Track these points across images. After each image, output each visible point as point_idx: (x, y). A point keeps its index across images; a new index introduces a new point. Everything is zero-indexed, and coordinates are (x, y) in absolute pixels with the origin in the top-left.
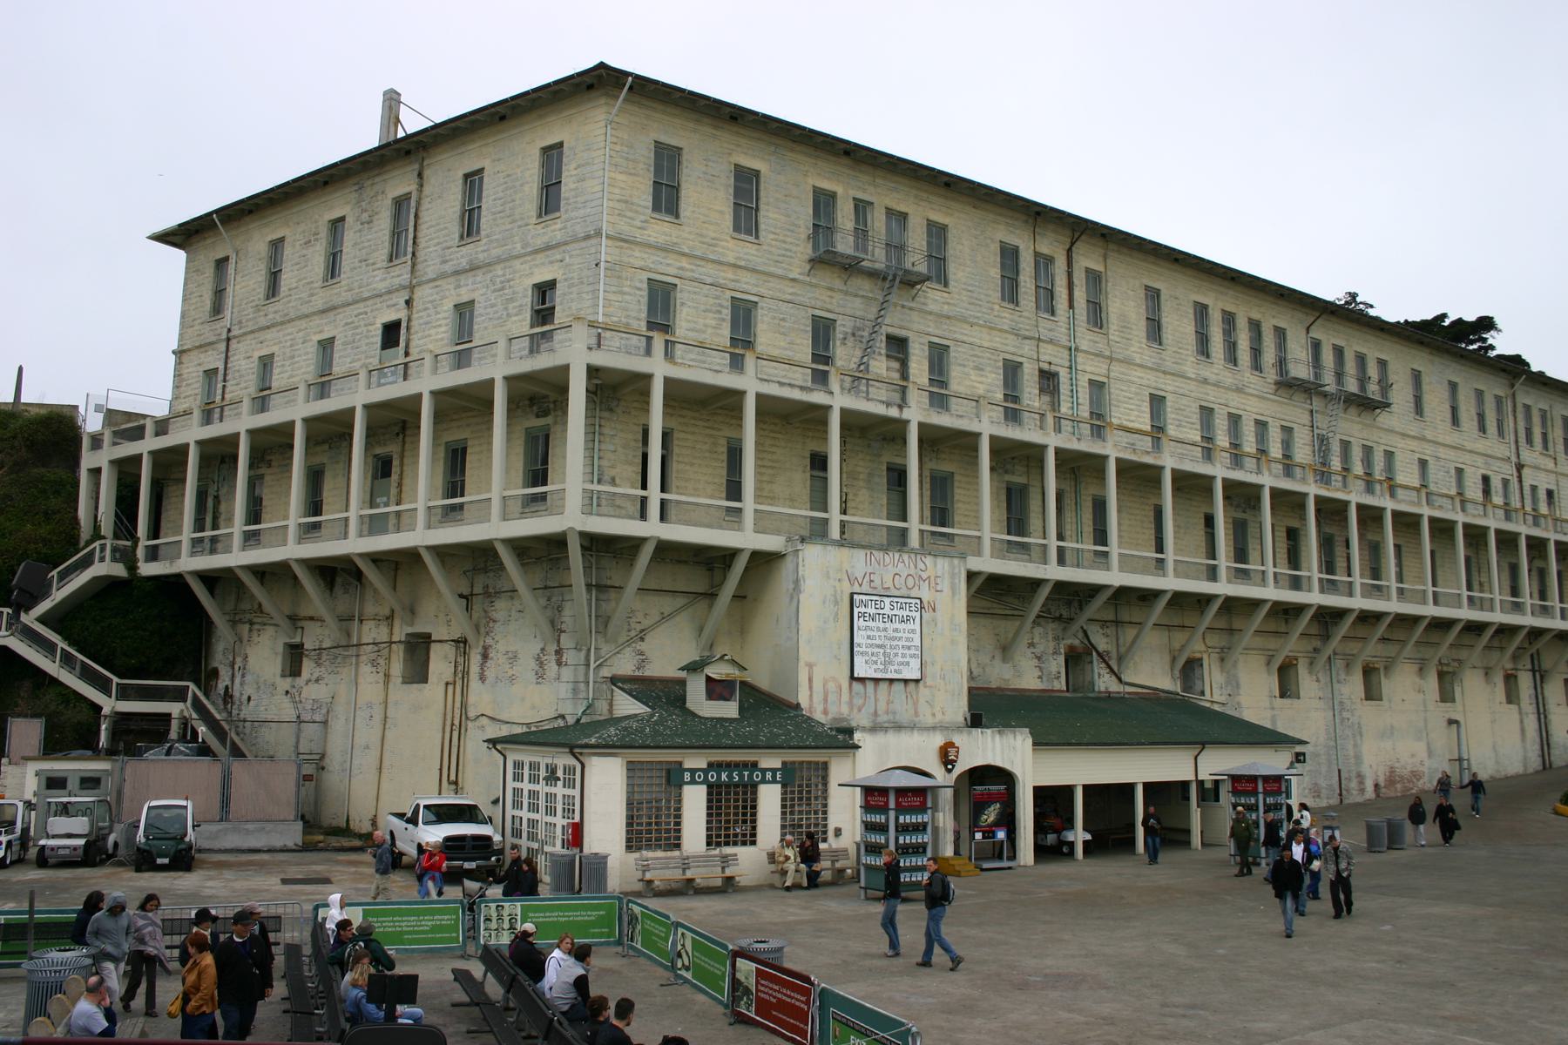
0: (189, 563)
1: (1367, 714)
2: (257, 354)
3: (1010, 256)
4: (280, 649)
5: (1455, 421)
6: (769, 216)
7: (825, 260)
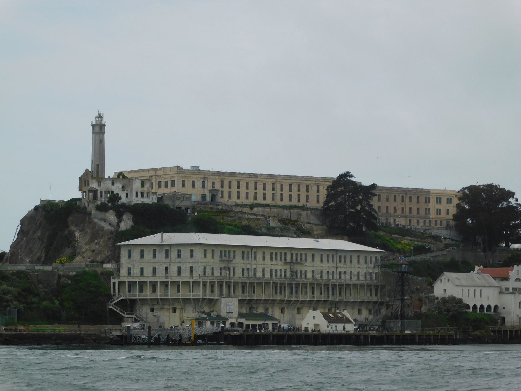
0: (137, 297)
1: (298, 316)
2: (140, 266)
3: (243, 252)
4: (149, 309)
5: (322, 261)
6: (215, 256)
7: (221, 260)
